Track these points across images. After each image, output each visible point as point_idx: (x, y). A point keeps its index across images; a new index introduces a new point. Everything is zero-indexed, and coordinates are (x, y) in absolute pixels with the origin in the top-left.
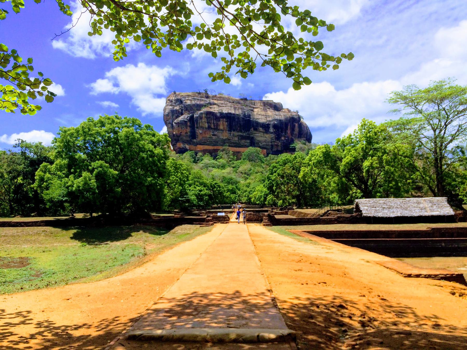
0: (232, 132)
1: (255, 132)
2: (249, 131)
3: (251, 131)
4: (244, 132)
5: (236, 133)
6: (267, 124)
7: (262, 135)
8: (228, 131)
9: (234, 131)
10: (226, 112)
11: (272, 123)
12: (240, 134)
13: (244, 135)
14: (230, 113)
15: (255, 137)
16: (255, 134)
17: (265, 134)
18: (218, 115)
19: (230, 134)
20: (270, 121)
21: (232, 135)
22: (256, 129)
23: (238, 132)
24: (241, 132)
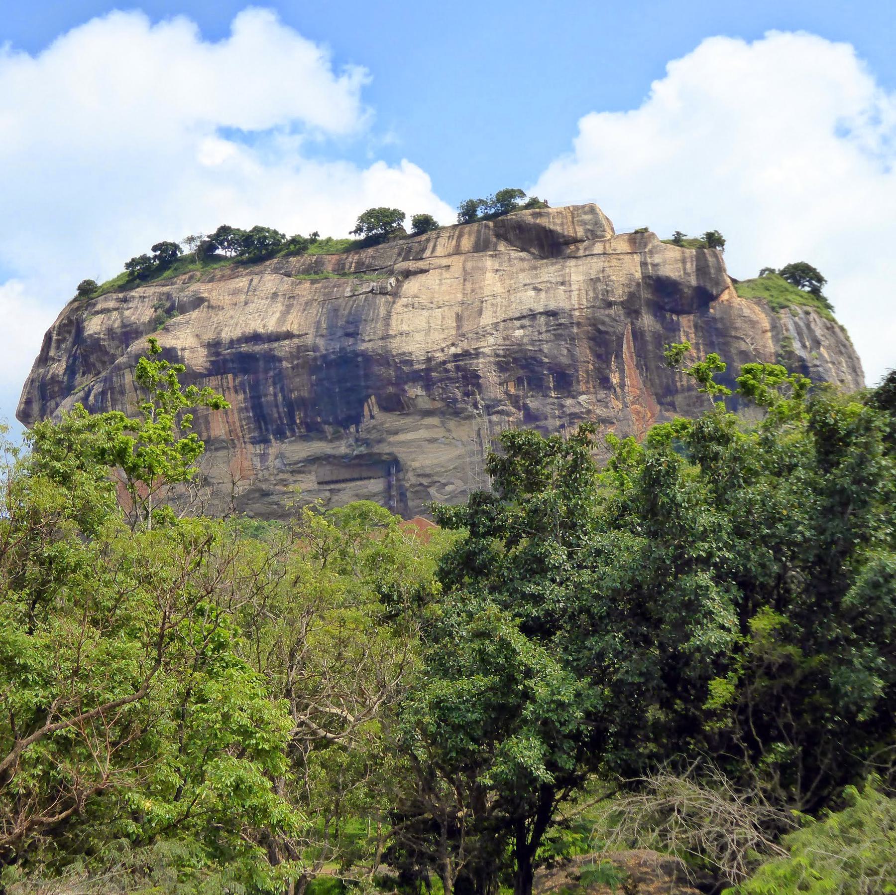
0: (275, 448)
1: (390, 420)
2: (356, 419)
3: (366, 422)
4: (337, 437)
5: (298, 450)
6: (456, 356)
7: (439, 433)
8: (254, 442)
9: (280, 435)
10: (237, 333)
11: (490, 344)
12: (318, 447)
13: (342, 448)
14: (256, 338)
15: (402, 454)
16: (396, 433)
17: (452, 424)
18: (198, 359)
19: (263, 457)
20: (480, 335)
21: (272, 462)
22: (395, 404)
23: (304, 438)
24: (322, 437)
